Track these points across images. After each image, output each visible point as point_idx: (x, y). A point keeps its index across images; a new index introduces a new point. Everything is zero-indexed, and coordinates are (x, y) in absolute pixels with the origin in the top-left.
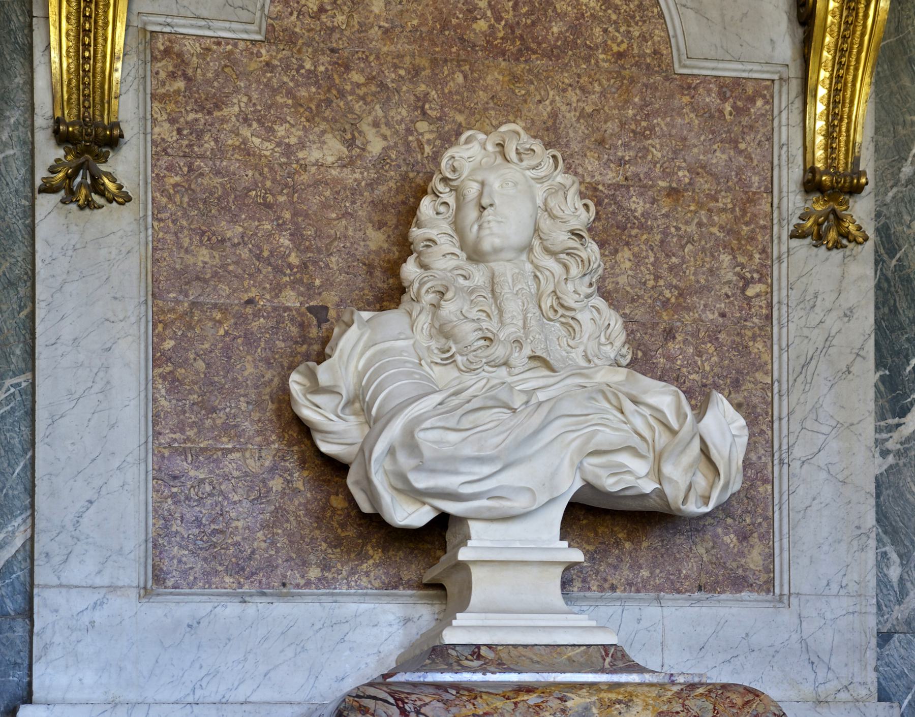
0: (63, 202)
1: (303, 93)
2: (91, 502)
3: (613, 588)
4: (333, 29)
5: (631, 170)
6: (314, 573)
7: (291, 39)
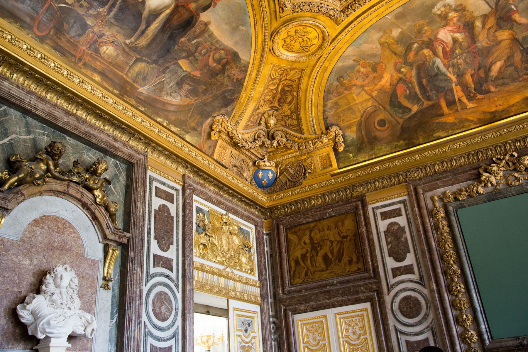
1: (24, 251)
7: (24, 241)
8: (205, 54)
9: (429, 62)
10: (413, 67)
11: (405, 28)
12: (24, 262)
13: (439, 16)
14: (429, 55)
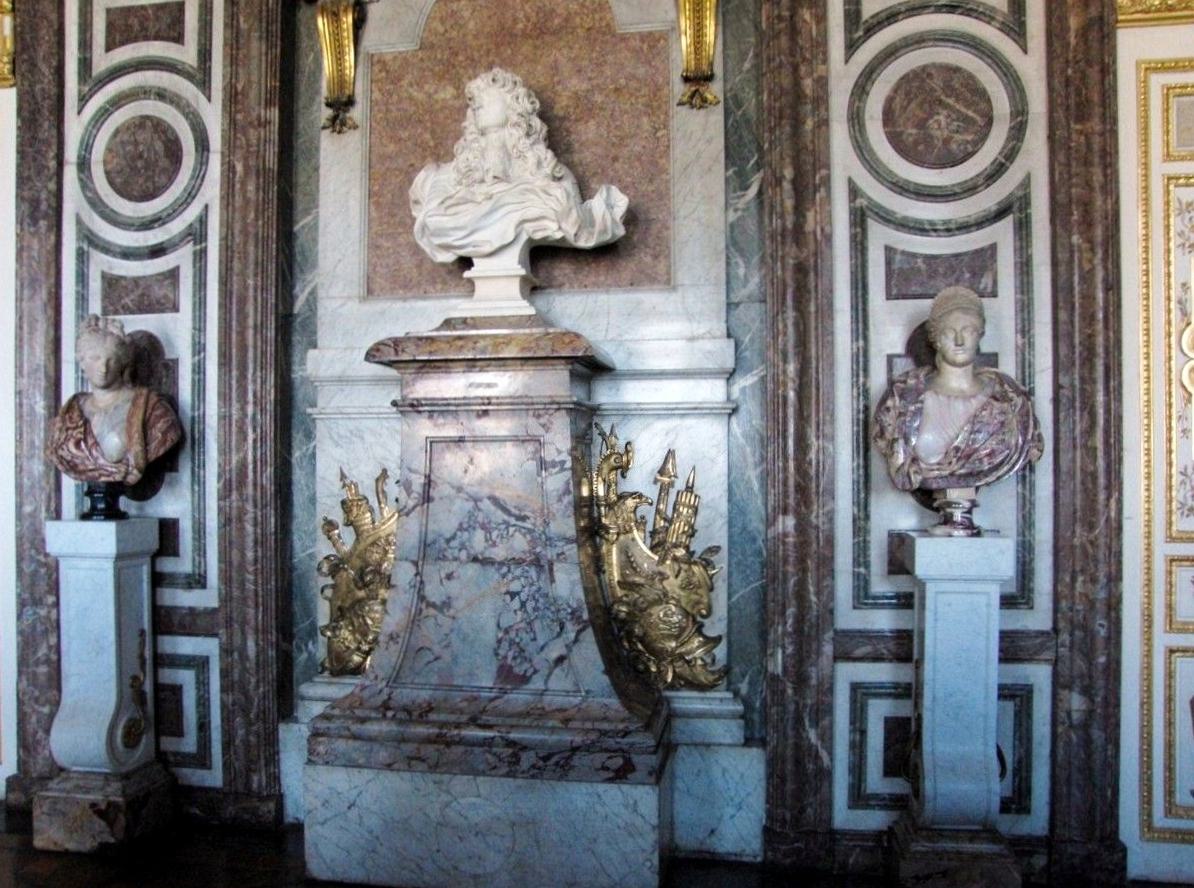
0: (333, 131)
2: (340, 261)
3: (586, 286)
4: (450, 39)
5: (595, 82)
6: (439, 286)
7: (432, 46)
12: (441, 95)
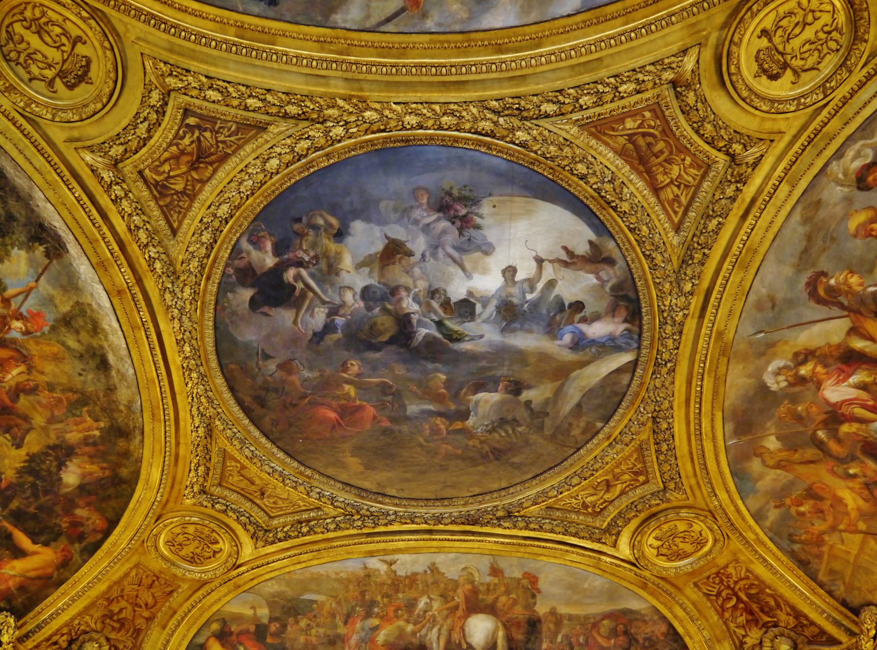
8: (587, 641)
9: (871, 436)
10: (859, 458)
11: (773, 431)
13: (791, 385)
14: (858, 429)
